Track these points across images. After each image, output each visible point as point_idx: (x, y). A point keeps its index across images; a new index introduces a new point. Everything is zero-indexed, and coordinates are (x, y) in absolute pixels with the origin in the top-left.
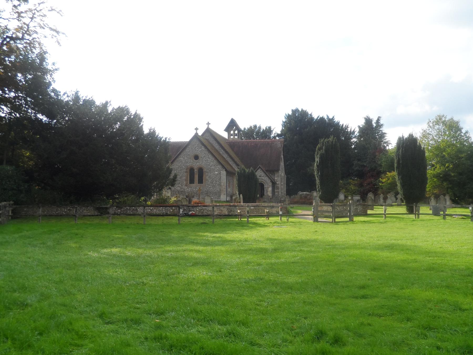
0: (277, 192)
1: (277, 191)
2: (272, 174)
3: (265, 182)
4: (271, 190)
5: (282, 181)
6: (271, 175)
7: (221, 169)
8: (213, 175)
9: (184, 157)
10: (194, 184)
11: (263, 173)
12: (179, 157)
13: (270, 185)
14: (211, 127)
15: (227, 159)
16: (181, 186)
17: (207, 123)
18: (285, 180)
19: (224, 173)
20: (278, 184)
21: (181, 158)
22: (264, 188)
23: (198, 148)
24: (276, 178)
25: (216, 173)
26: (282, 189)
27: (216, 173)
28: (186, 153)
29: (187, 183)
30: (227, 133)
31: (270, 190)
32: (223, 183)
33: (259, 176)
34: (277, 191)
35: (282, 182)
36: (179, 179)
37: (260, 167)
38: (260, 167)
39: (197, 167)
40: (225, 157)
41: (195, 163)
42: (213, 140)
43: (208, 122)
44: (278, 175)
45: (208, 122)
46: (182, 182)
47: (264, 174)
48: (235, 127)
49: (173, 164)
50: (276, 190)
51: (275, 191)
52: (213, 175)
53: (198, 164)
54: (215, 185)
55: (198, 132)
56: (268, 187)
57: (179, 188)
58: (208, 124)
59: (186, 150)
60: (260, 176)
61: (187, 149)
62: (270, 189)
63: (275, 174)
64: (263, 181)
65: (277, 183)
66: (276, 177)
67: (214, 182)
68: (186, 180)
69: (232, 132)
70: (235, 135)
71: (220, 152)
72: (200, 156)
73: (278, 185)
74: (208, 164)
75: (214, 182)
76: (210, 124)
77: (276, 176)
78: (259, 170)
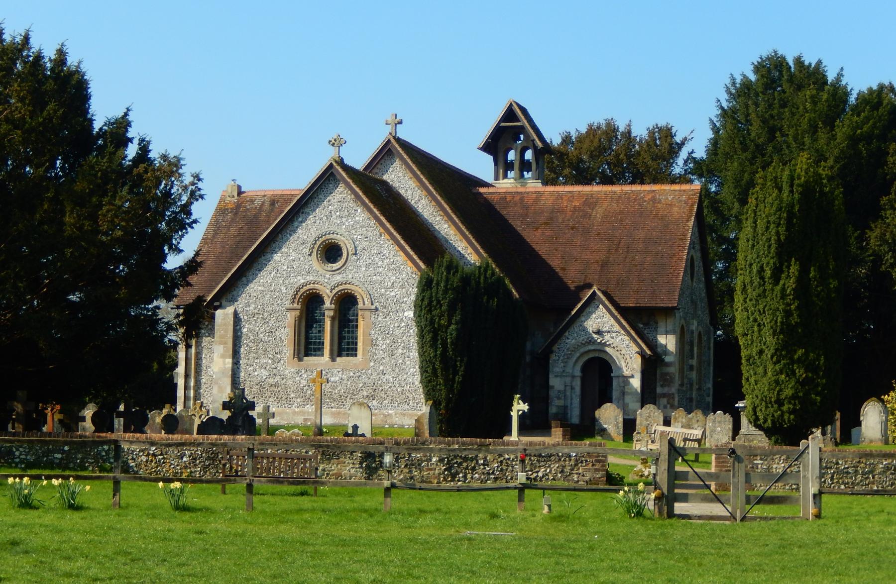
0: (664, 395)
1: (666, 390)
5: (692, 350)
6: (641, 326)
10: (322, 355)
13: (635, 366)
18: (709, 349)
22: (611, 378)
26: (691, 385)
27: (406, 314)
30: (490, 159)
34: (666, 390)
35: (692, 358)
41: (327, 276)
48: (522, 137)
50: (662, 386)
51: (659, 390)
54: (404, 362)
63: (657, 323)
69: (512, 155)
70: (525, 166)
75: (400, 351)
76: (400, 122)
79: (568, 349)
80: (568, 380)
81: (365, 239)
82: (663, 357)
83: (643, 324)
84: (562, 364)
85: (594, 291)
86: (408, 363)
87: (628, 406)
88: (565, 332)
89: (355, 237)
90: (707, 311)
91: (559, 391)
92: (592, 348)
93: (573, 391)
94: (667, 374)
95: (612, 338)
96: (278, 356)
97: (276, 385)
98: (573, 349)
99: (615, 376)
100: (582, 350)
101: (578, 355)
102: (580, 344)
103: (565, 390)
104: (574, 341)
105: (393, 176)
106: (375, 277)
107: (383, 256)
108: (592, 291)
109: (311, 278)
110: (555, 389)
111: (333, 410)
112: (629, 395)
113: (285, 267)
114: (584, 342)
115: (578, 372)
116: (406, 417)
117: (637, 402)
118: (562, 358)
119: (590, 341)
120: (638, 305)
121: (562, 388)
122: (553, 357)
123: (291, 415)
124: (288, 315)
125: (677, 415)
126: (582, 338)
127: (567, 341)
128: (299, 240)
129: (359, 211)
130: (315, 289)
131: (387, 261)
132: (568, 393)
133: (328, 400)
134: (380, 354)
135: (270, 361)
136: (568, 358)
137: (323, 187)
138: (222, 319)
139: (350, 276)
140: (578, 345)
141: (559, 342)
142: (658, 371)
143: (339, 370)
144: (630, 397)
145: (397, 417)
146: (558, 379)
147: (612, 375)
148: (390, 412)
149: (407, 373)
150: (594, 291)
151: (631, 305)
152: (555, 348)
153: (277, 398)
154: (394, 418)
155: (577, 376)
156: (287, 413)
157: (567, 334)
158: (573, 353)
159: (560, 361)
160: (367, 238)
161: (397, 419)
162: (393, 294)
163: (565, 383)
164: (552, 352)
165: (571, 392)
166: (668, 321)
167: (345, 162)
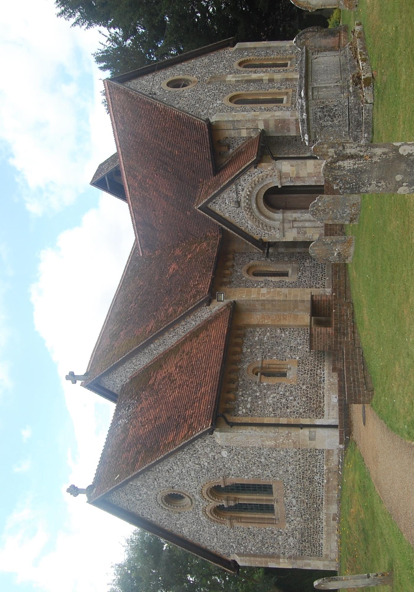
1: (293, 127)
2: (229, 147)
3: (258, 188)
4: (292, 166)
5: (254, 81)
6: (231, 150)
7: (207, 442)
8: (236, 462)
9: (178, 526)
10: (273, 505)
11: (225, 195)
12: (181, 535)
14: (81, 370)
15: (183, 334)
16: (285, 535)
17: (70, 382)
19: (219, 437)
20: (266, 122)
21: (185, 532)
23: (140, 495)
24: (244, 133)
25: (224, 454)
26: (287, 80)
28: (162, 521)
29: (272, 522)
31: (294, 168)
32: (263, 441)
33: (239, 206)
34: (293, 127)
35: (262, 80)
36: (260, 538)
37: (205, 208)
38: (205, 208)
39: (208, 499)
40: (175, 338)
42: (121, 369)
43: (67, 378)
44: (230, 126)
45: (67, 378)
46: (270, 533)
47: (228, 190)
49: (209, 548)
50: (289, 131)
52: (236, 462)
53: (197, 497)
55: (85, 487)
56: (281, 177)
57: (289, 540)
58: (72, 377)
59: (154, 519)
60: (238, 203)
61: (149, 517)
62: (286, 167)
63: (227, 138)
64: (255, 192)
65: (261, 127)
66: (240, 133)
67: (263, 460)
68: (262, 521)
71: (160, 352)
72: (167, 491)
73: (272, 124)
74: (192, 472)
75: (263, 460)
77: (233, 133)
78: (216, 208)
79: (258, 227)
80: (287, 225)
81: (157, 480)
82: (259, 130)
83: (229, 149)
84: (273, 231)
85: (199, 208)
86: (274, 455)
87: (311, 173)
88: (241, 230)
89: (156, 486)
90: (221, 51)
91: (298, 233)
92: (255, 205)
93: (297, 219)
94: (276, 126)
95: (243, 190)
96: (275, 532)
97: (302, 535)
98: (257, 222)
99: (281, 185)
100: (257, 213)
101: (262, 217)
102: (252, 217)
103: (297, 227)
104: (249, 222)
105: (117, 380)
106: (192, 475)
107: (171, 470)
108: (199, 210)
109: (201, 512)
110: (297, 236)
111: (324, 502)
112: (298, 173)
113: (194, 526)
114: (250, 214)
115: (278, 216)
116: (331, 459)
117: (306, 165)
118: (266, 232)
119: (247, 208)
120: (210, 159)
121: (295, 231)
122: (266, 239)
123: (329, 528)
124: (238, 526)
125: (320, 154)
126: (246, 216)
127: (250, 227)
128: (167, 518)
129: (131, 483)
130: (210, 511)
131: (175, 468)
132: (300, 224)
133: (315, 505)
134: (267, 473)
135: (280, 537)
136: (266, 227)
137: (116, 503)
138: (245, 562)
139: (195, 490)
140: (253, 218)
141: (251, 234)
142: (274, 135)
143: (285, 498)
144: (300, 172)
145: (331, 465)
146: (287, 234)
147: (280, 187)
148: (325, 468)
149: (285, 456)
150: (199, 208)
151: (211, 165)
152: (257, 237)
153: (314, 534)
154: (331, 467)
155: (283, 216)
156: (328, 530)
157: (243, 228)
158: (261, 221)
159: (270, 233)
160: (156, 479)
161: (332, 464)
162: (206, 464)
163: (290, 228)
164: (261, 239)
165: (298, 221)
166: (223, 127)
167: (91, 483)
